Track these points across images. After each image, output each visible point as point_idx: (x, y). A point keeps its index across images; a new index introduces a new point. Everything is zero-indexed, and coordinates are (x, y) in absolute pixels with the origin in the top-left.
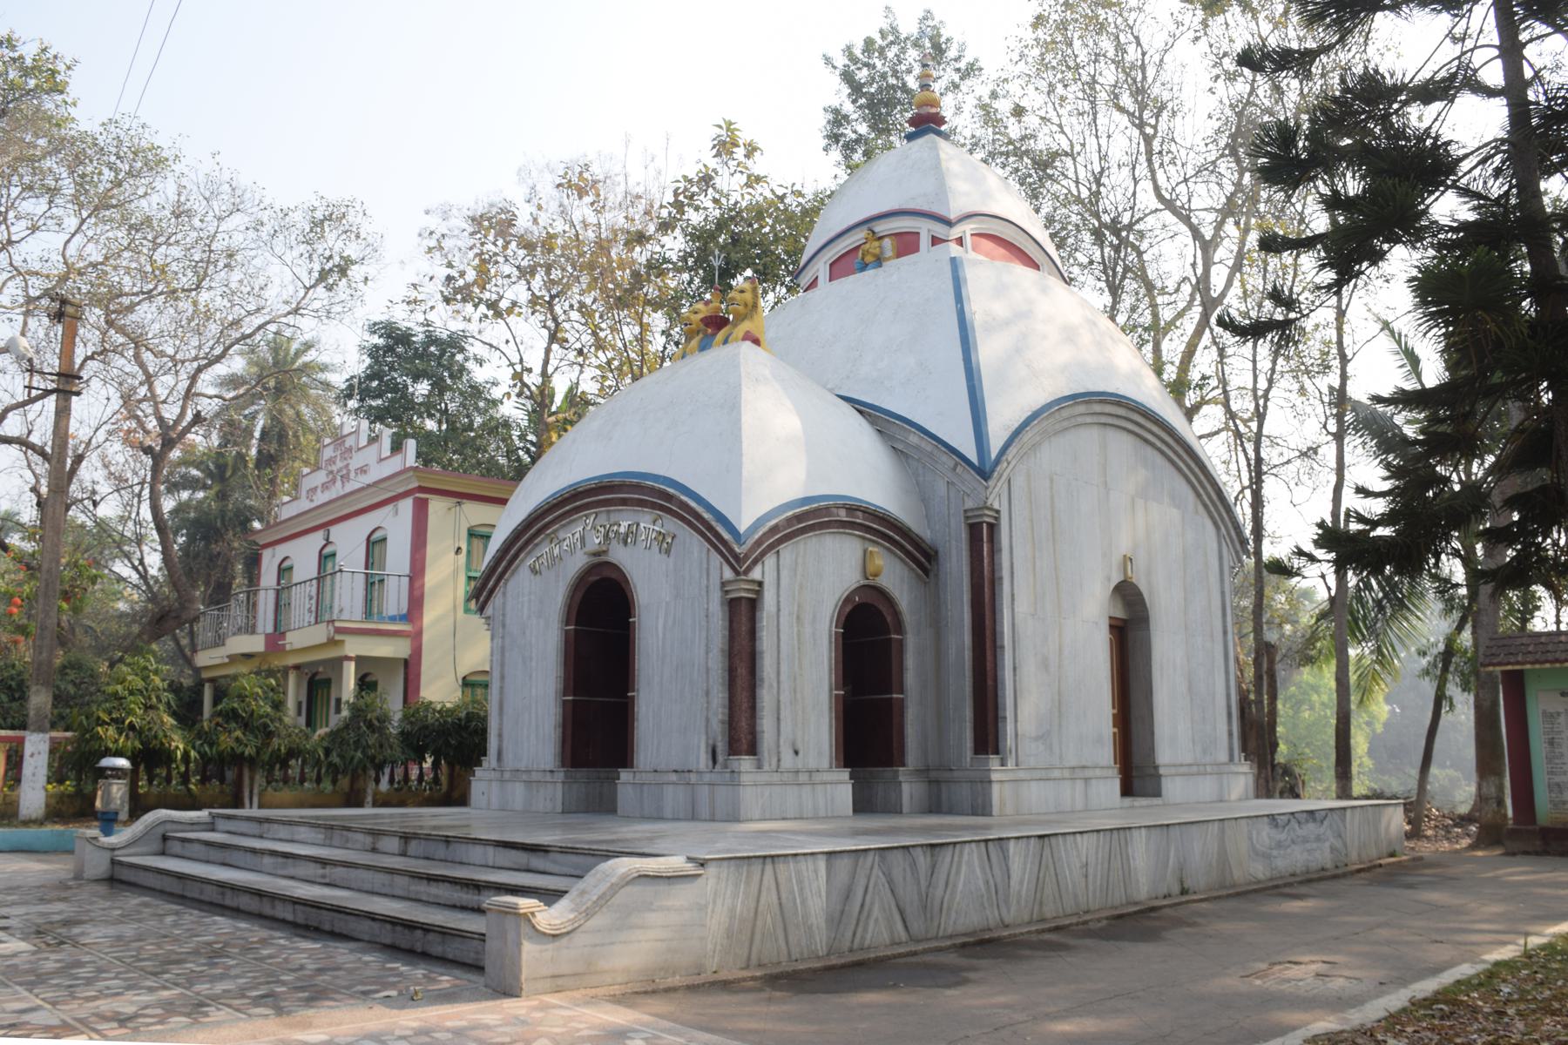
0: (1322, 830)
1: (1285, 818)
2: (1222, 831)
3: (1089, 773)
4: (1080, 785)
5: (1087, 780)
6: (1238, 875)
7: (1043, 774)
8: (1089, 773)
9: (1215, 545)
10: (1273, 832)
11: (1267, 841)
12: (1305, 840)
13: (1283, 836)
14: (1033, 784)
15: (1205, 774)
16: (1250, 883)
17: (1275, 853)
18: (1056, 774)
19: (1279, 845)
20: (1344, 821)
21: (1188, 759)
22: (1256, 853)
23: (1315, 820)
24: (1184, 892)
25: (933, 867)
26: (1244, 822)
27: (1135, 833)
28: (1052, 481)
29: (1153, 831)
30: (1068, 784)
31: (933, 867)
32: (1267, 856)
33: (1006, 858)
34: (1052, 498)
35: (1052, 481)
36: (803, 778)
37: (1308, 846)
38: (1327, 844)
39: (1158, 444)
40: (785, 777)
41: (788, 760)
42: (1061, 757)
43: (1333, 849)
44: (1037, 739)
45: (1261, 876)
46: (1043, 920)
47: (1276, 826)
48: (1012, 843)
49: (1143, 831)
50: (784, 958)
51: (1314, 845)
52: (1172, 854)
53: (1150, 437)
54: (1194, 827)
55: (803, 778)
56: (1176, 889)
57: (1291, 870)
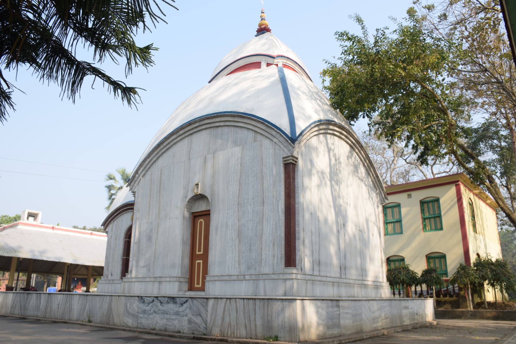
0: (181, 309)
1: (151, 299)
2: (111, 300)
3: (162, 280)
4: (156, 284)
5: (160, 282)
6: (117, 321)
7: (142, 280)
8: (162, 280)
9: (271, 151)
10: (141, 305)
11: (136, 309)
12: (165, 313)
13: (148, 308)
14: (136, 284)
15: (245, 279)
16: (124, 326)
17: (141, 315)
18: (148, 279)
19: (144, 312)
20: (206, 306)
21: (234, 272)
22: (129, 313)
23: (175, 303)
24: (90, 321)
25: (27, 298)
26: (123, 298)
27: (75, 296)
28: (161, 171)
29: (81, 296)
30: (151, 283)
31: (27, 298)
32: (135, 316)
33: (40, 298)
34: (161, 177)
35: (161, 171)
36: (111, 282)
37: (168, 316)
38: (186, 318)
39: (222, 124)
40: (108, 282)
41: (110, 277)
42: (153, 273)
43: (190, 322)
44: (143, 267)
45: (130, 324)
46: (46, 318)
47: (144, 302)
48: (42, 295)
49: (78, 296)
50: (20, 313)
51: (173, 317)
52: (87, 306)
53: (217, 124)
54: (98, 297)
55: (111, 282)
56: (87, 320)
57: (152, 328)
